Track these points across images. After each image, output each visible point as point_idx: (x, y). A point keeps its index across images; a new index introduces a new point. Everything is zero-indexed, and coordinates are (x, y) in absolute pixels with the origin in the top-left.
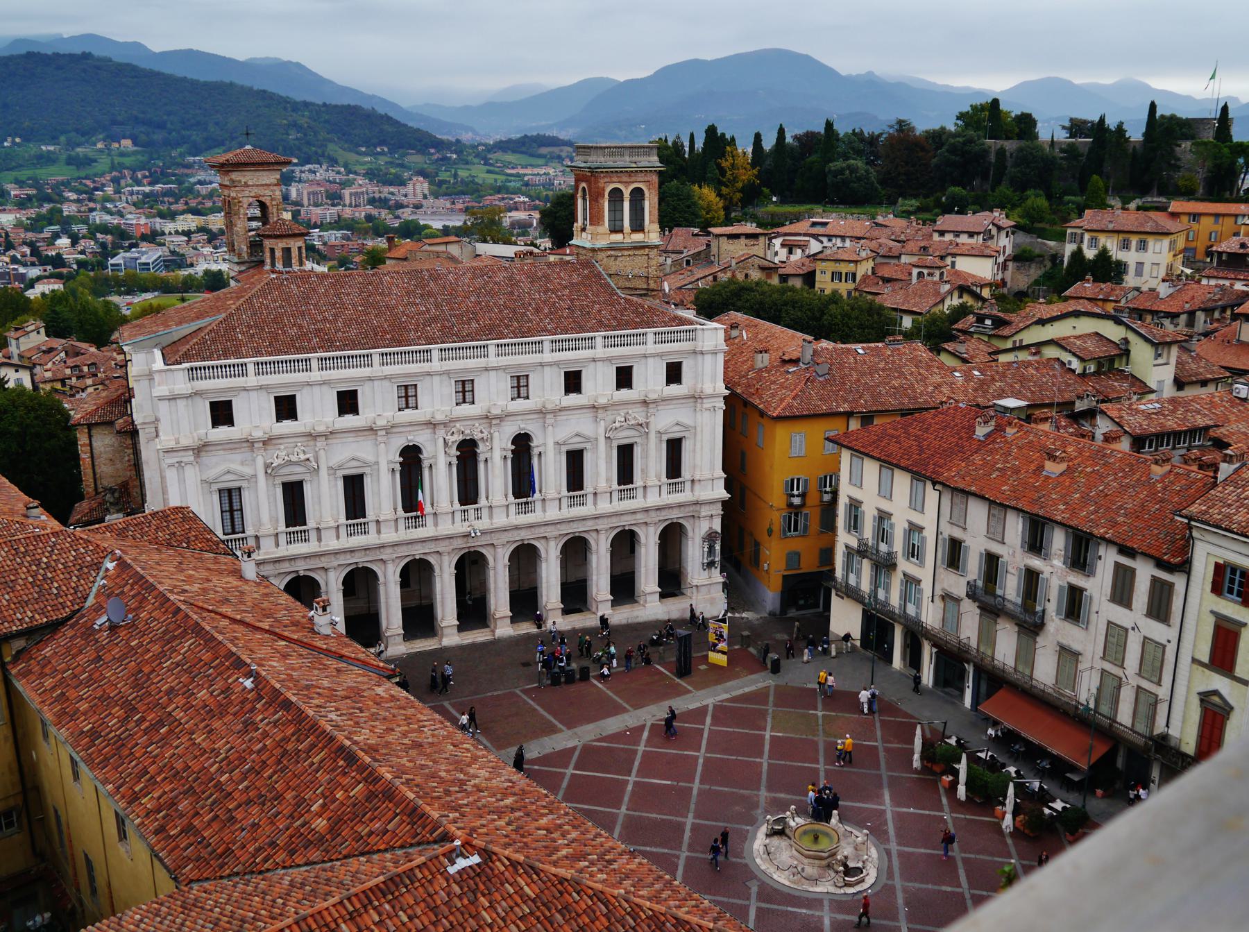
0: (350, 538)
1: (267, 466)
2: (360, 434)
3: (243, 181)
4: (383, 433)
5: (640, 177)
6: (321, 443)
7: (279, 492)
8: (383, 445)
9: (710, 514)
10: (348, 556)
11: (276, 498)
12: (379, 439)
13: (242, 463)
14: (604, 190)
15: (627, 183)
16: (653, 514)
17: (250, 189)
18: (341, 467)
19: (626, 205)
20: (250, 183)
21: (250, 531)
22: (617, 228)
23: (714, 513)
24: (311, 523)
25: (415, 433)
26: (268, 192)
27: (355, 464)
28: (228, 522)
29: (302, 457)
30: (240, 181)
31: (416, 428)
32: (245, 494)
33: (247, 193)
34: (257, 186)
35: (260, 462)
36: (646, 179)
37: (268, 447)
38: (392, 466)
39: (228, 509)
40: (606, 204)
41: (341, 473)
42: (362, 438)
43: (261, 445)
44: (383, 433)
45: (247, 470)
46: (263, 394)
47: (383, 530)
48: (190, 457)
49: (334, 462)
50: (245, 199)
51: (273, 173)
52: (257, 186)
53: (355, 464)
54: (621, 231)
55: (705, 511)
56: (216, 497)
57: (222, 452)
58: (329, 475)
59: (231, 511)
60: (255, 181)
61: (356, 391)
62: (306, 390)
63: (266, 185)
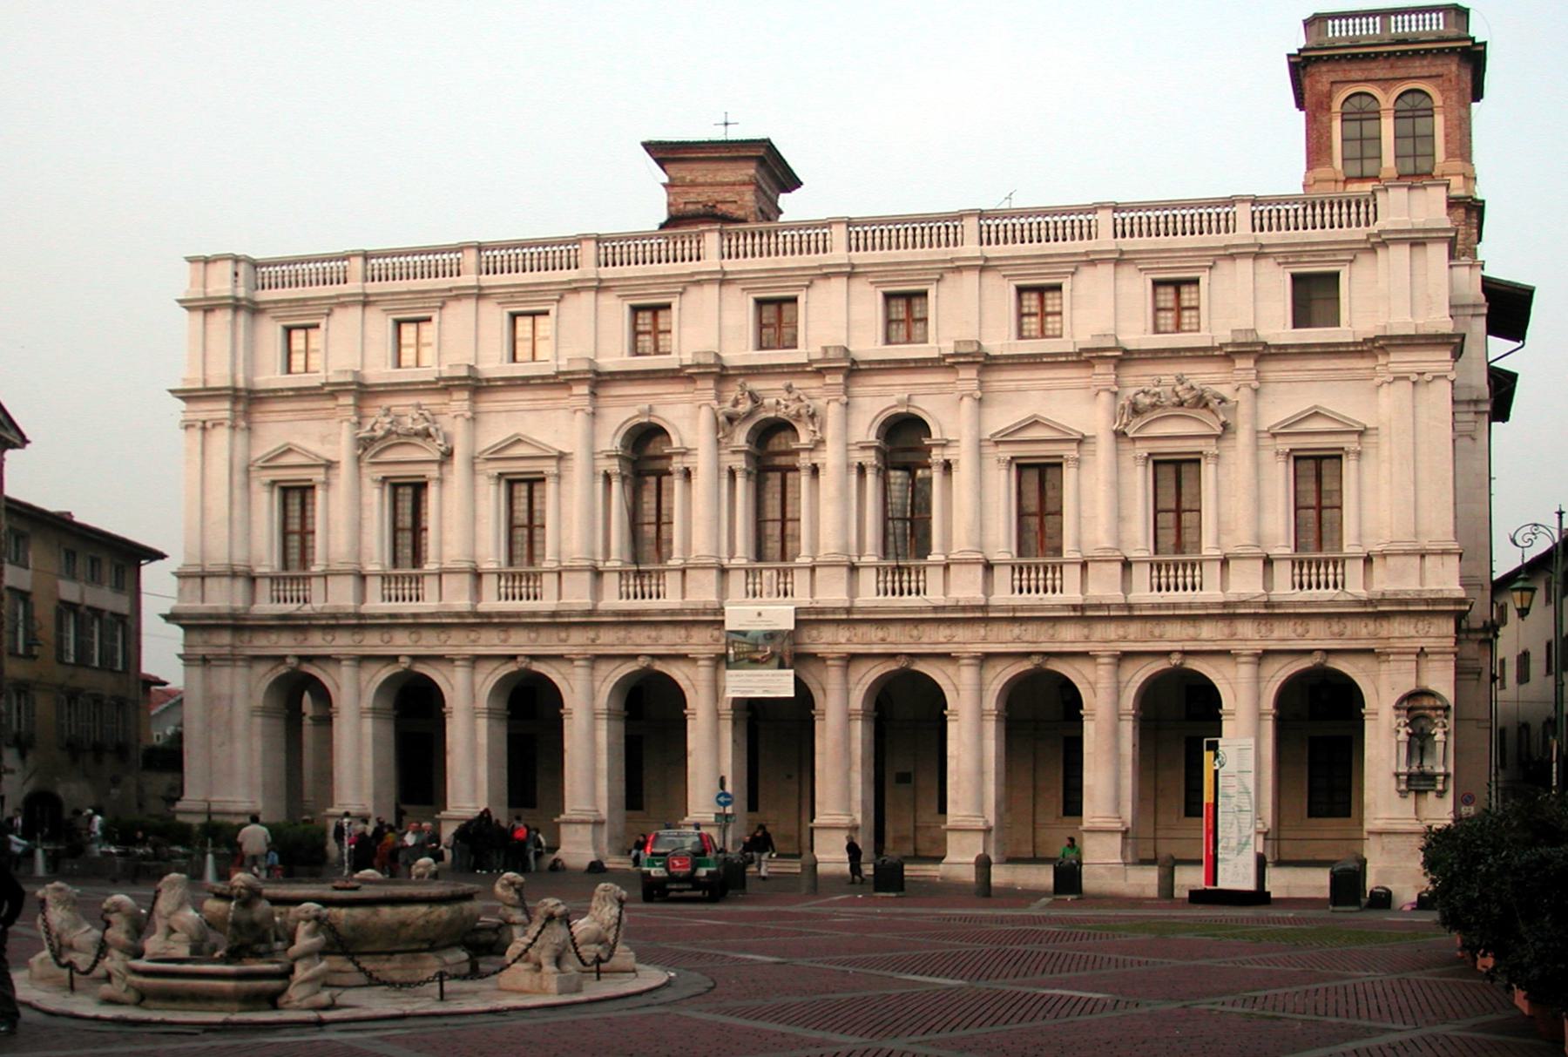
3: (688, 178)
5: (1419, 67)
9: (1423, 643)
14: (1330, 96)
15: (1385, 82)
16: (1246, 629)
17: (699, 189)
19: (1387, 126)
20: (701, 180)
22: (1368, 171)
23: (1426, 643)
26: (729, 196)
30: (684, 178)
34: (711, 185)
36: (1434, 71)
40: (1337, 125)
51: (742, 165)
52: (711, 185)
54: (1376, 178)
55: (1400, 631)
63: (727, 184)
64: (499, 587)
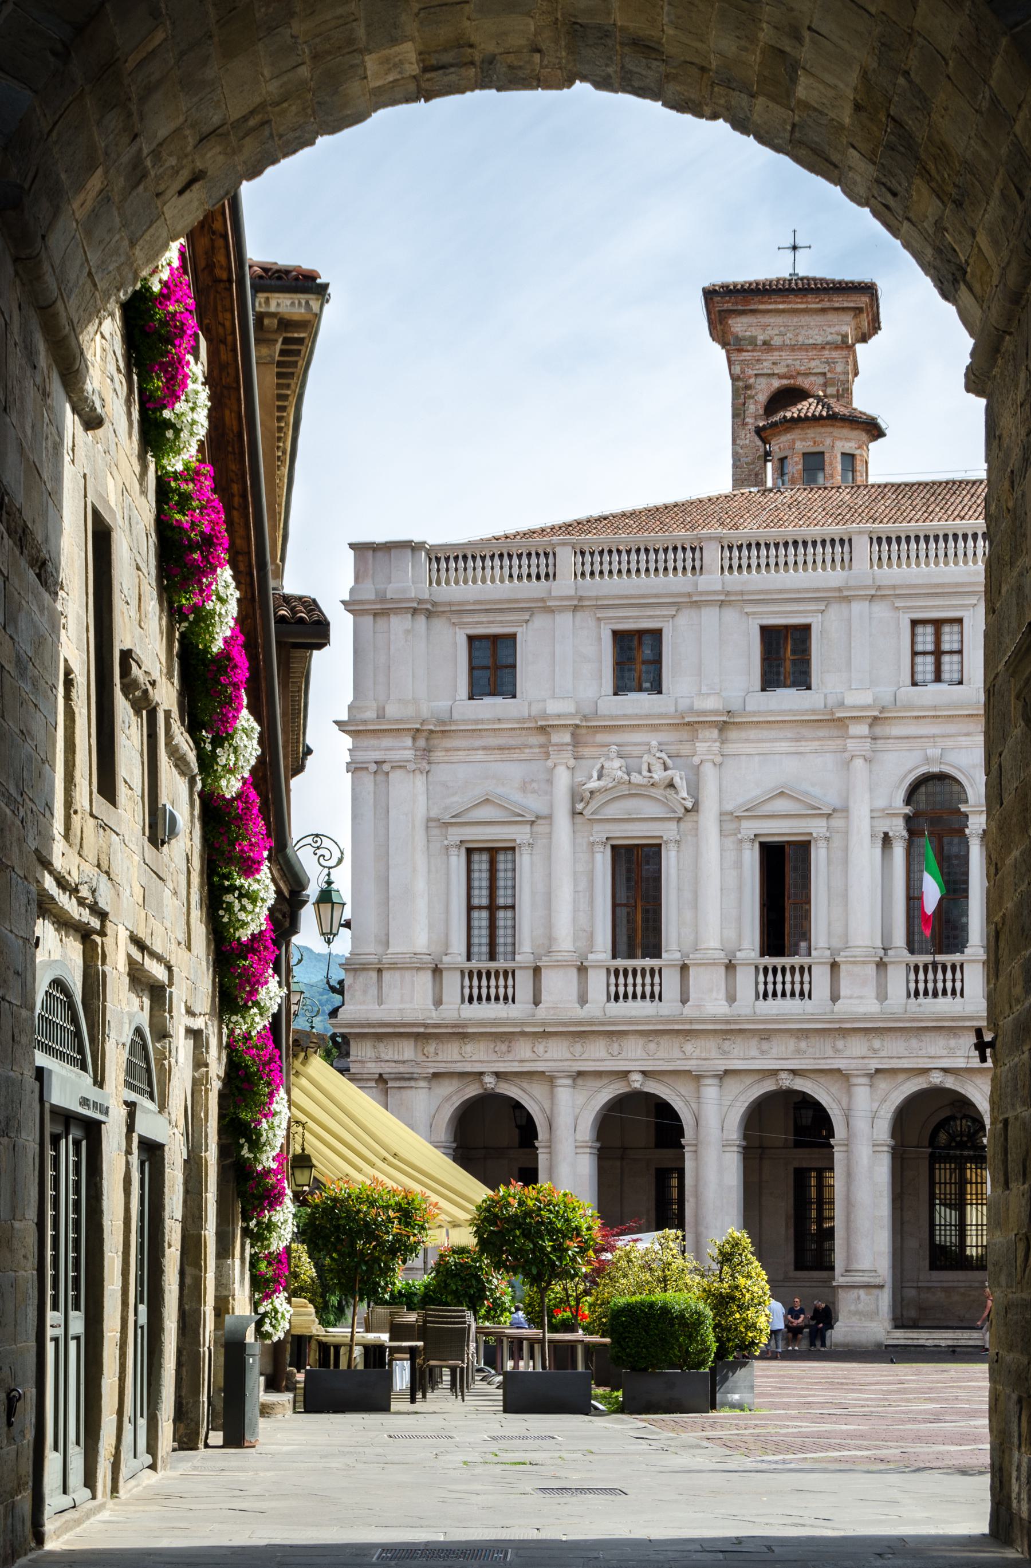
0: (761, 1002)
1: (576, 796)
2: (805, 732)
3: (761, 338)
4: (863, 729)
6: (706, 745)
7: (603, 862)
8: (859, 762)
10: (752, 1048)
11: (591, 882)
12: (851, 744)
13: (524, 788)
17: (775, 356)
18: (751, 813)
20: (777, 341)
21: (525, 955)
24: (671, 952)
25: (949, 743)
27: (782, 806)
28: (481, 937)
29: (659, 775)
31: (951, 728)
32: (524, 860)
33: (766, 367)
34: (793, 348)
35: (563, 780)
37: (586, 751)
38: (883, 826)
39: (485, 902)
41: (750, 828)
42: (814, 745)
43: (567, 738)
44: (863, 729)
45: (534, 804)
46: (586, 620)
47: (845, 989)
48: (403, 749)
49: (738, 798)
50: (762, 381)
51: (832, 317)
52: (793, 348)
53: (782, 806)
56: (458, 862)
57: (480, 755)
58: (722, 833)
59: (492, 908)
60: (789, 338)
61: (806, 628)
62: (685, 619)
64: (757, 983)
